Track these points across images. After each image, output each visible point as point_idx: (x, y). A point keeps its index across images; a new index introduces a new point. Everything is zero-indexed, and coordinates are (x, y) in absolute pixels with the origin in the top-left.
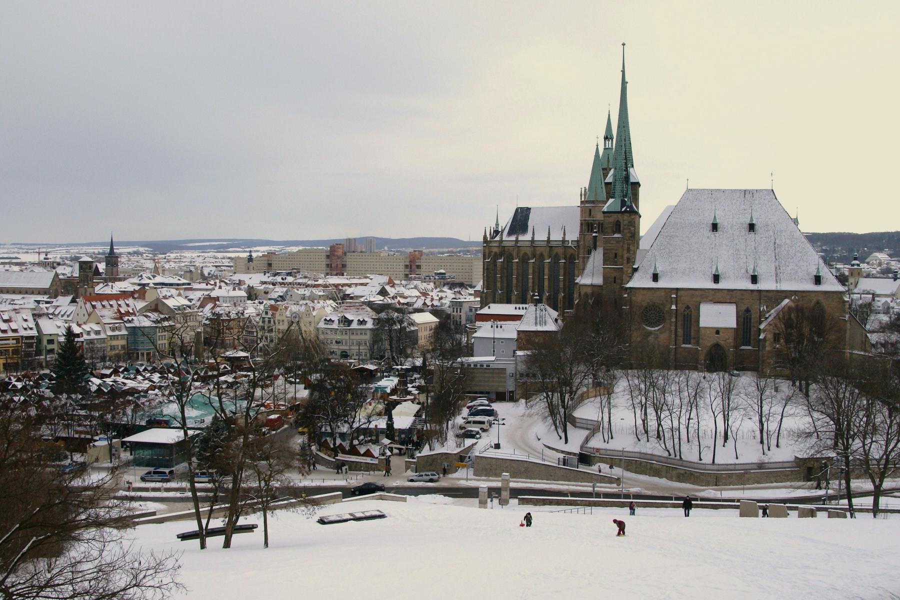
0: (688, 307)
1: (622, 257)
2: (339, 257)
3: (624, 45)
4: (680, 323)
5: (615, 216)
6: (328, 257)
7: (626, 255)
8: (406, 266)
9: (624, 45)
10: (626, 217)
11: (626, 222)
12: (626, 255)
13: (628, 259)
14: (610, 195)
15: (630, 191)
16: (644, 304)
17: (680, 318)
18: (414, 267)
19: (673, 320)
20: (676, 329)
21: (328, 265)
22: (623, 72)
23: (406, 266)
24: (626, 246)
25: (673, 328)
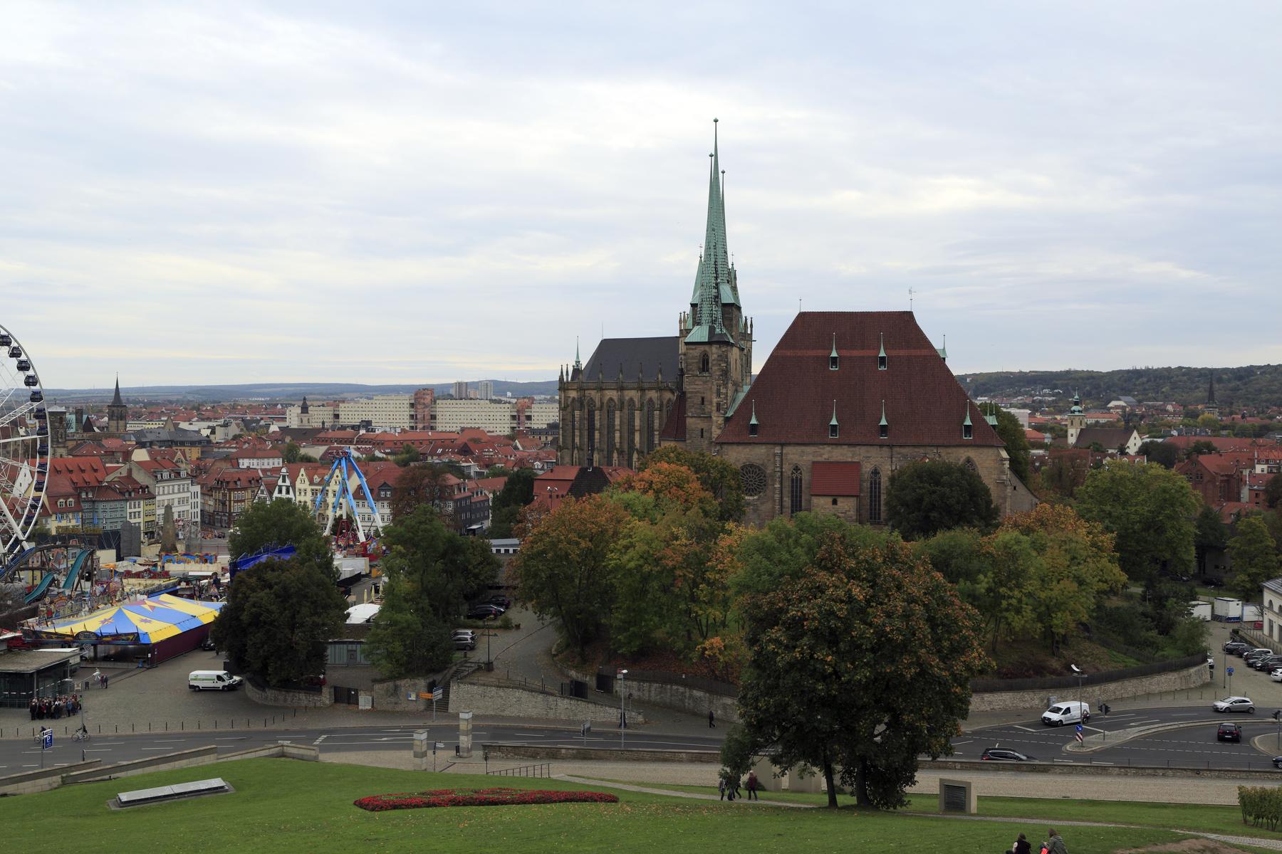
0: (797, 469)
1: (711, 403)
2: (426, 406)
3: (716, 121)
4: (787, 491)
5: (702, 348)
6: (412, 405)
7: (715, 400)
8: (513, 417)
9: (716, 121)
10: (714, 349)
11: (715, 356)
12: (715, 400)
13: (718, 405)
14: (696, 322)
15: (719, 315)
16: (739, 466)
17: (787, 483)
18: (523, 418)
19: (777, 486)
20: (782, 498)
21: (412, 416)
22: (715, 156)
23: (513, 417)
24: (715, 388)
25: (777, 496)
